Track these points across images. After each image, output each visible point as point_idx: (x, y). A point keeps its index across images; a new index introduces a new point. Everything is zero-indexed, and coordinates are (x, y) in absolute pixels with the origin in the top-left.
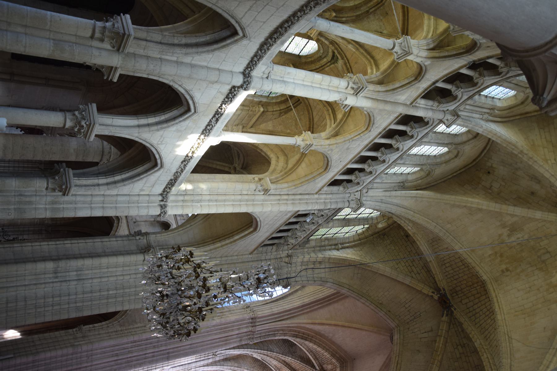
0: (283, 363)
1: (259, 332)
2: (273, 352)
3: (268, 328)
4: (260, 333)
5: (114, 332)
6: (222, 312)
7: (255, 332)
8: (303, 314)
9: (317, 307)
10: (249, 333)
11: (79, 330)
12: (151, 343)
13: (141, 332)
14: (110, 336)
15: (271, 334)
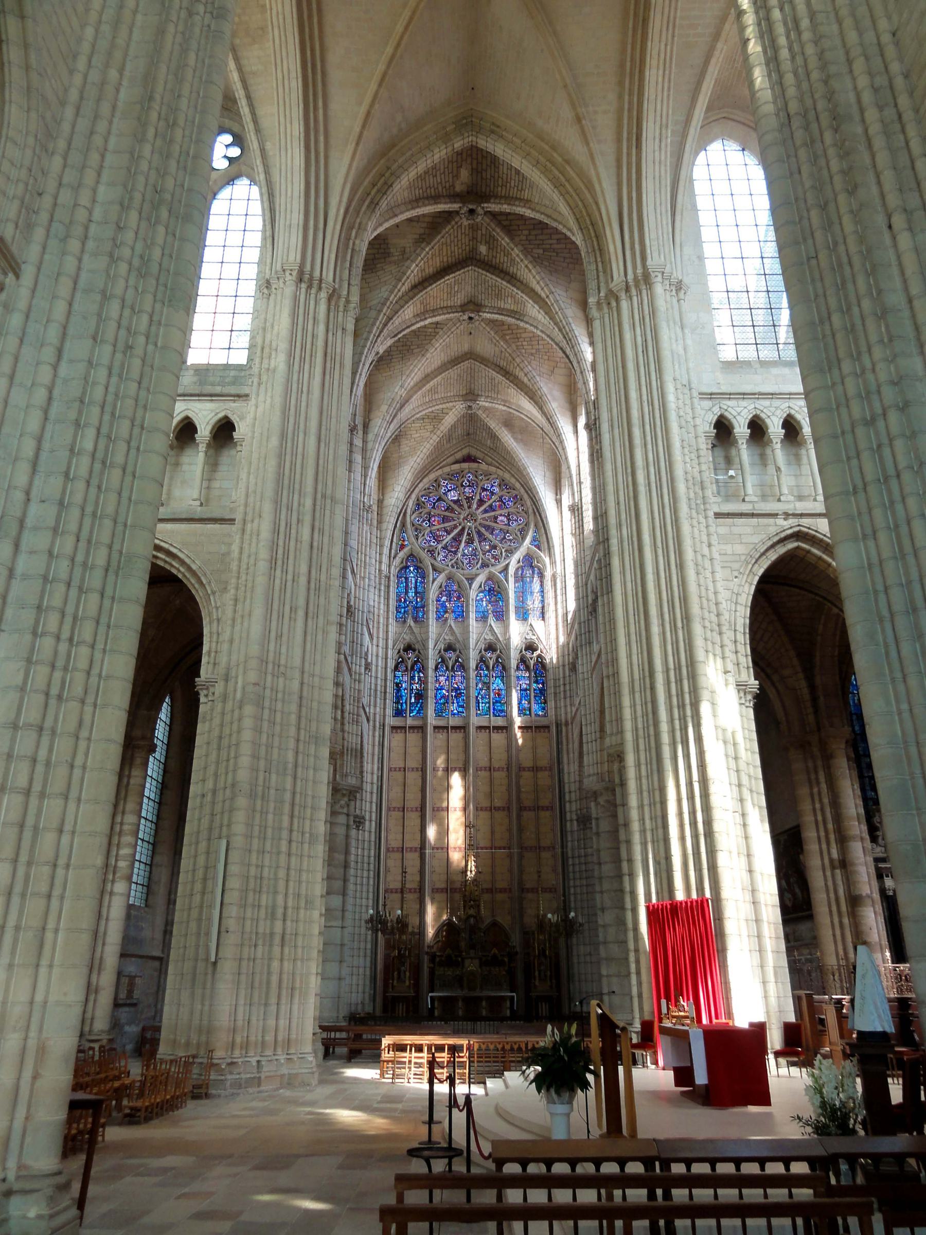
0: (416, 291)
1: (337, 280)
2: (387, 299)
3: (333, 256)
4: (341, 280)
5: (235, 605)
6: (263, 349)
7: (334, 290)
8: (326, 158)
9: (321, 112)
10: (333, 303)
11: (207, 689)
12: (288, 525)
13: (254, 540)
14: (242, 617)
15: (352, 257)
